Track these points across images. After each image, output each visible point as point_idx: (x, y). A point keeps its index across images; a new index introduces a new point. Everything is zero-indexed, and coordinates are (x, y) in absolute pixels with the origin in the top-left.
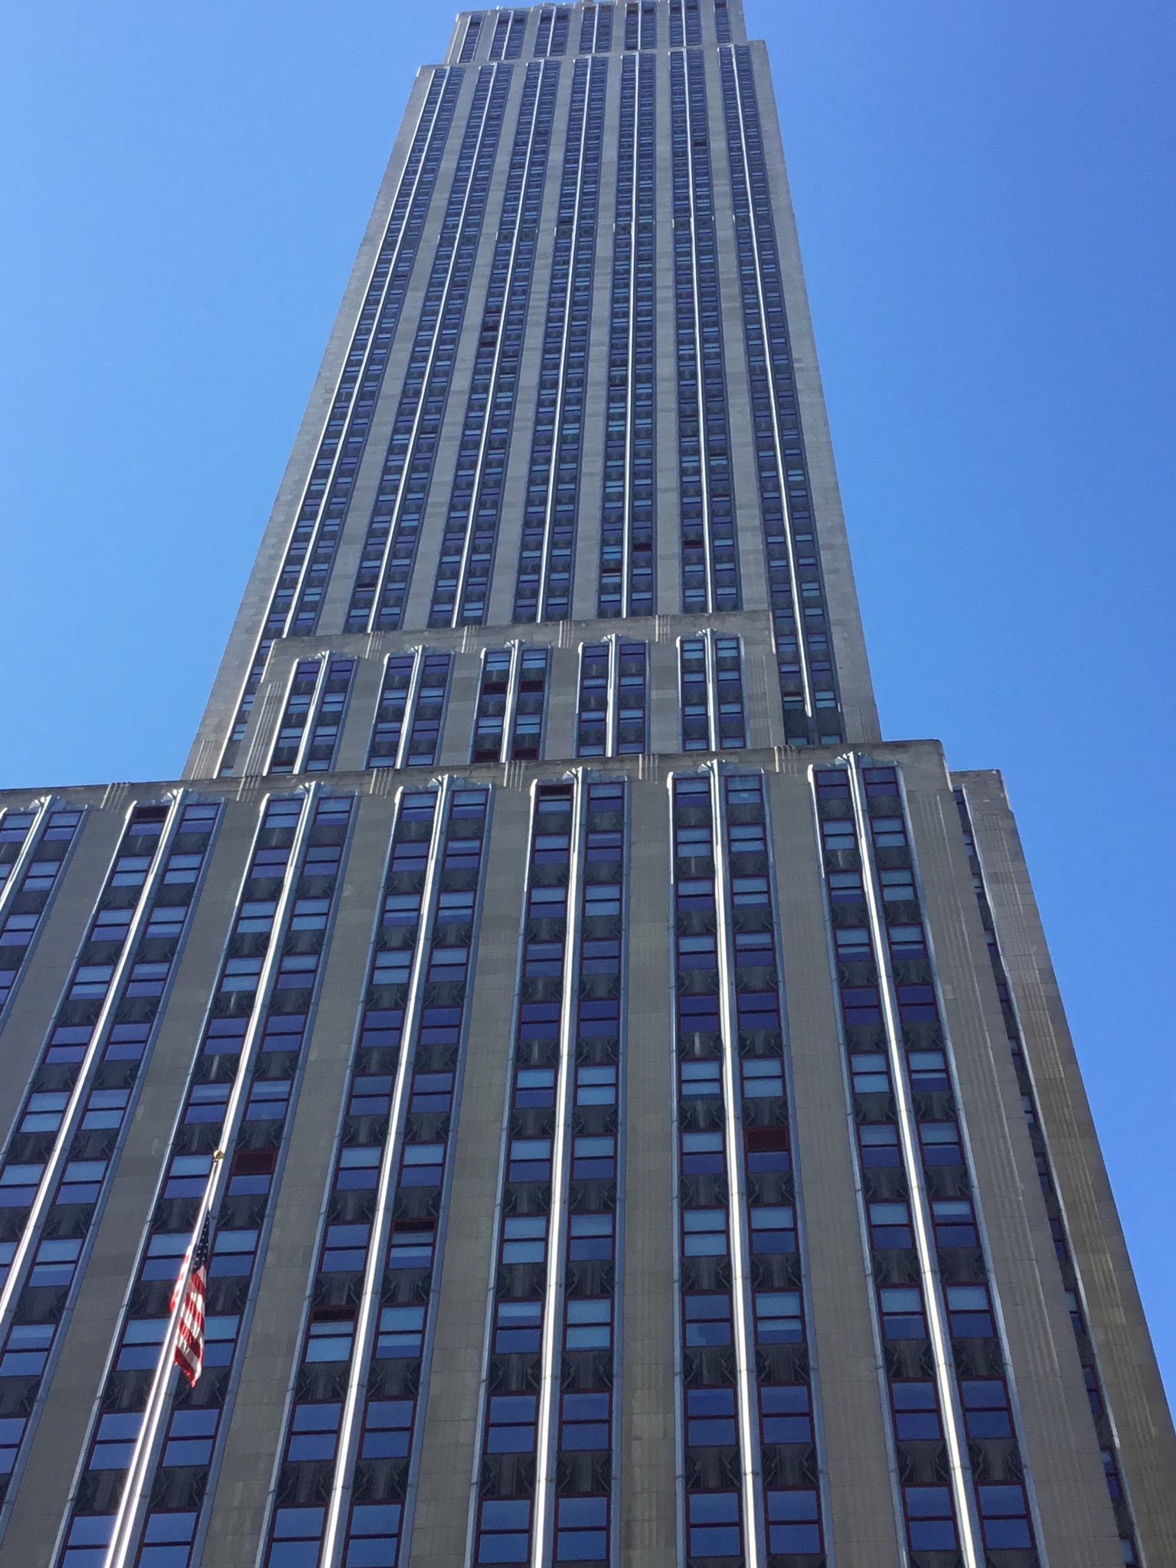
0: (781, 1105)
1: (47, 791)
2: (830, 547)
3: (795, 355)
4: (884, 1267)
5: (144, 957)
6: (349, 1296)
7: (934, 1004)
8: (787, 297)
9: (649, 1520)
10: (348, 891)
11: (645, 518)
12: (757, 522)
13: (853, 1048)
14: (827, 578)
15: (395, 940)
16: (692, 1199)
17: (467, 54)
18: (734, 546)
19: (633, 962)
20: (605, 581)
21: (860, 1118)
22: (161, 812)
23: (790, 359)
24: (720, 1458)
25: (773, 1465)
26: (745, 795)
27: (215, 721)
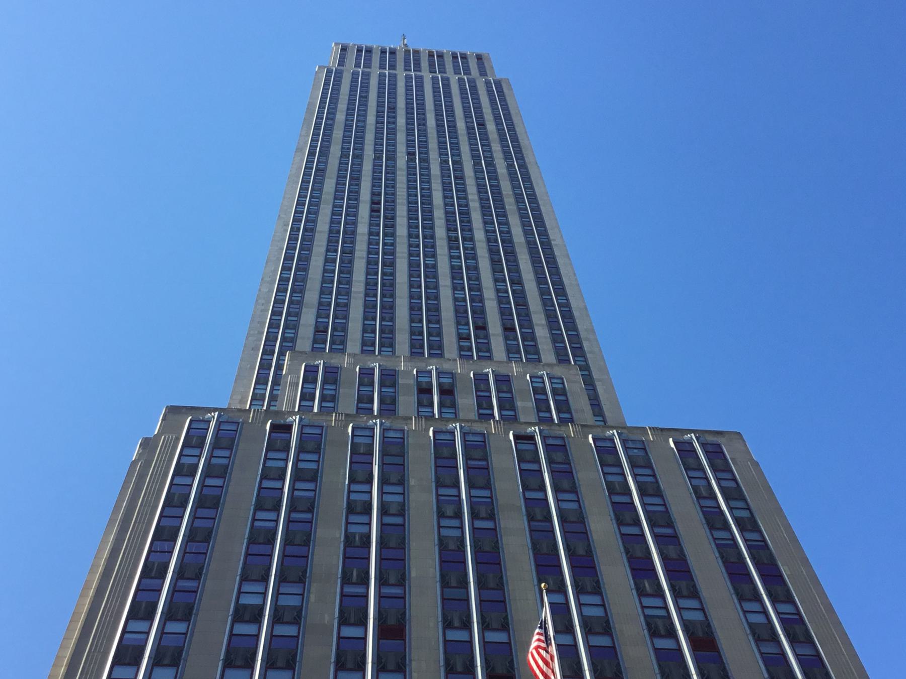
0: (707, 624)
1: (215, 410)
2: (588, 340)
5: (295, 508)
7: (781, 576)
8: (542, 208)
10: (412, 482)
11: (480, 313)
12: (544, 322)
13: (741, 598)
14: (588, 355)
15: (449, 511)
17: (342, 62)
18: (533, 333)
19: (595, 537)
20: (462, 344)
21: (756, 636)
22: (288, 428)
23: (548, 238)
26: (636, 451)
27: (239, 397)
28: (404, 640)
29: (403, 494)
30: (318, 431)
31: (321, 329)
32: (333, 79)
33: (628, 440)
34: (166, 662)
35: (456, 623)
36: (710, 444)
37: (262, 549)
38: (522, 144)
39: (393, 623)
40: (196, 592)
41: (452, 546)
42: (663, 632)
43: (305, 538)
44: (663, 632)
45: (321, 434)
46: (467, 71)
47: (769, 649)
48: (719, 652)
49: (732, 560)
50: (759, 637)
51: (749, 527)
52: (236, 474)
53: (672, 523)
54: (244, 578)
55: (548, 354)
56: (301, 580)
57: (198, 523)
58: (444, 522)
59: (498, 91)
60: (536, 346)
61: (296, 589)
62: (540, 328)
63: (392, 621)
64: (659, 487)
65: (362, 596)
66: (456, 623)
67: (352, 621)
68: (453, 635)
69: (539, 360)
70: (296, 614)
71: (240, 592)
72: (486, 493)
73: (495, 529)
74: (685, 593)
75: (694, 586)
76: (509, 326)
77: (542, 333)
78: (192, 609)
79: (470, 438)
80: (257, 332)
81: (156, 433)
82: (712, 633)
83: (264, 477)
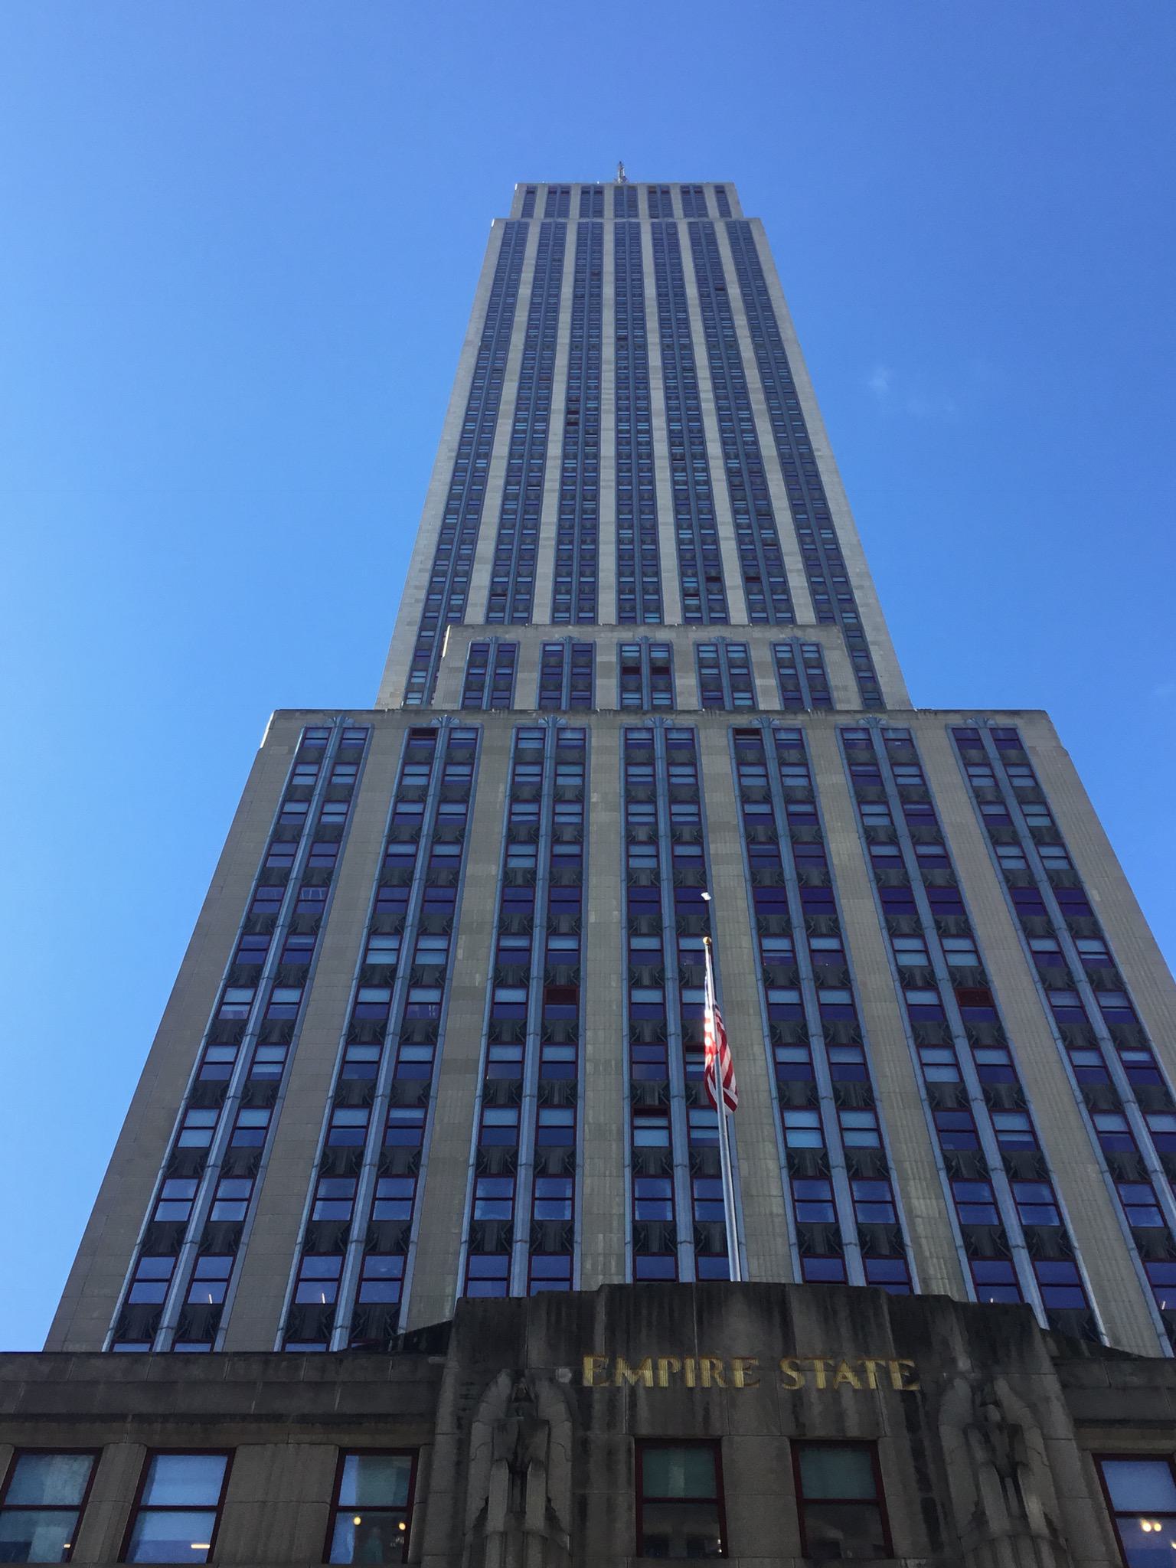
0: (980, 971)
3: (814, 446)
4: (1091, 1097)
6: (659, 1098)
8: (802, 404)
9: (942, 1278)
10: (594, 798)
12: (801, 566)
14: (860, 610)
15: (642, 834)
16: (923, 1038)
17: (528, 210)
18: (785, 583)
19: (836, 861)
20: (687, 602)
23: (810, 448)
24: (991, 1236)
25: (1034, 1241)
28: (577, 1003)
29: (582, 814)
30: (471, 735)
31: (499, 591)
32: (513, 237)
33: (888, 729)
34: (274, 1038)
35: (646, 981)
36: (1002, 729)
37: (398, 893)
38: (776, 314)
39: (562, 983)
40: (312, 950)
41: (644, 881)
42: (920, 983)
43: (451, 877)
44: (920, 983)
45: (476, 739)
46: (703, 210)
47: (1064, 1000)
48: (993, 1006)
49: (1021, 884)
50: (1050, 985)
51: (1047, 839)
52: (363, 797)
53: (942, 838)
54: (374, 931)
55: (805, 612)
56: (446, 932)
57: (315, 863)
58: (636, 850)
59: (742, 236)
60: (788, 601)
61: (440, 943)
62: (795, 574)
63: (562, 981)
64: (927, 792)
65: (525, 950)
66: (646, 981)
67: (510, 981)
68: (642, 996)
69: (792, 620)
70: (438, 975)
71: (367, 950)
72: (692, 809)
73: (702, 857)
74: (953, 930)
75: (967, 921)
76: (752, 575)
77: (797, 581)
78: (307, 971)
79: (674, 735)
80: (413, 601)
81: (261, 746)
82: (987, 983)
83: (400, 798)
